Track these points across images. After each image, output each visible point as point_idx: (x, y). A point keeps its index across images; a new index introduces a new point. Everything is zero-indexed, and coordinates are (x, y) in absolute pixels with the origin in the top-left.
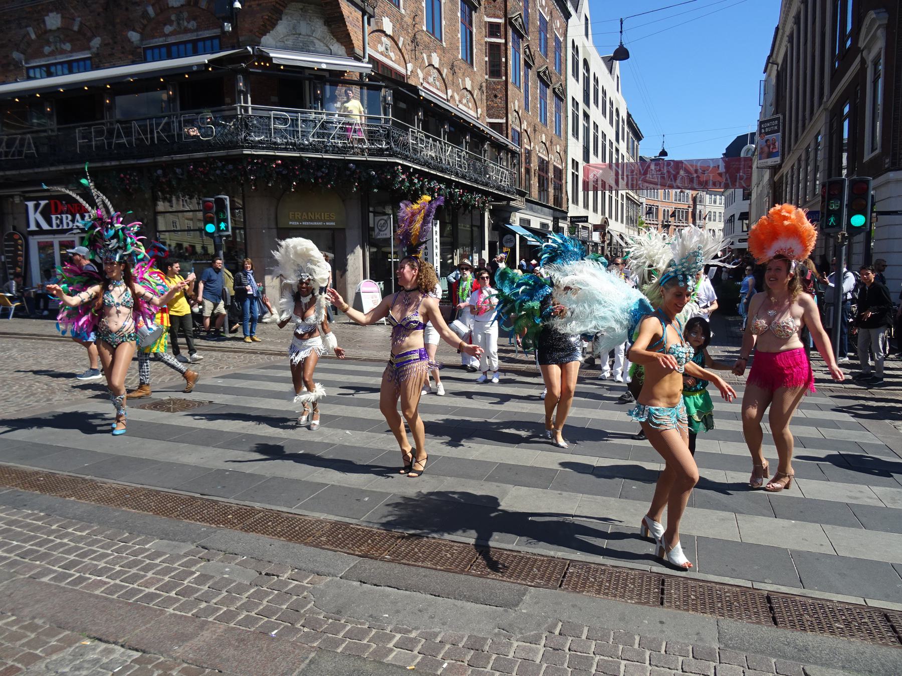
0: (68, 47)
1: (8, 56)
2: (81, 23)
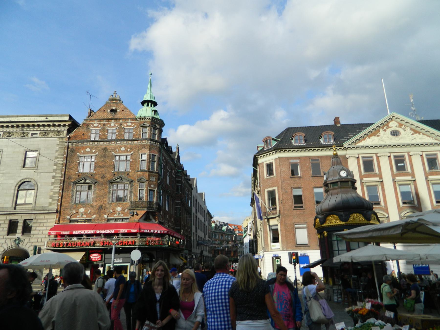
0: (85, 216)
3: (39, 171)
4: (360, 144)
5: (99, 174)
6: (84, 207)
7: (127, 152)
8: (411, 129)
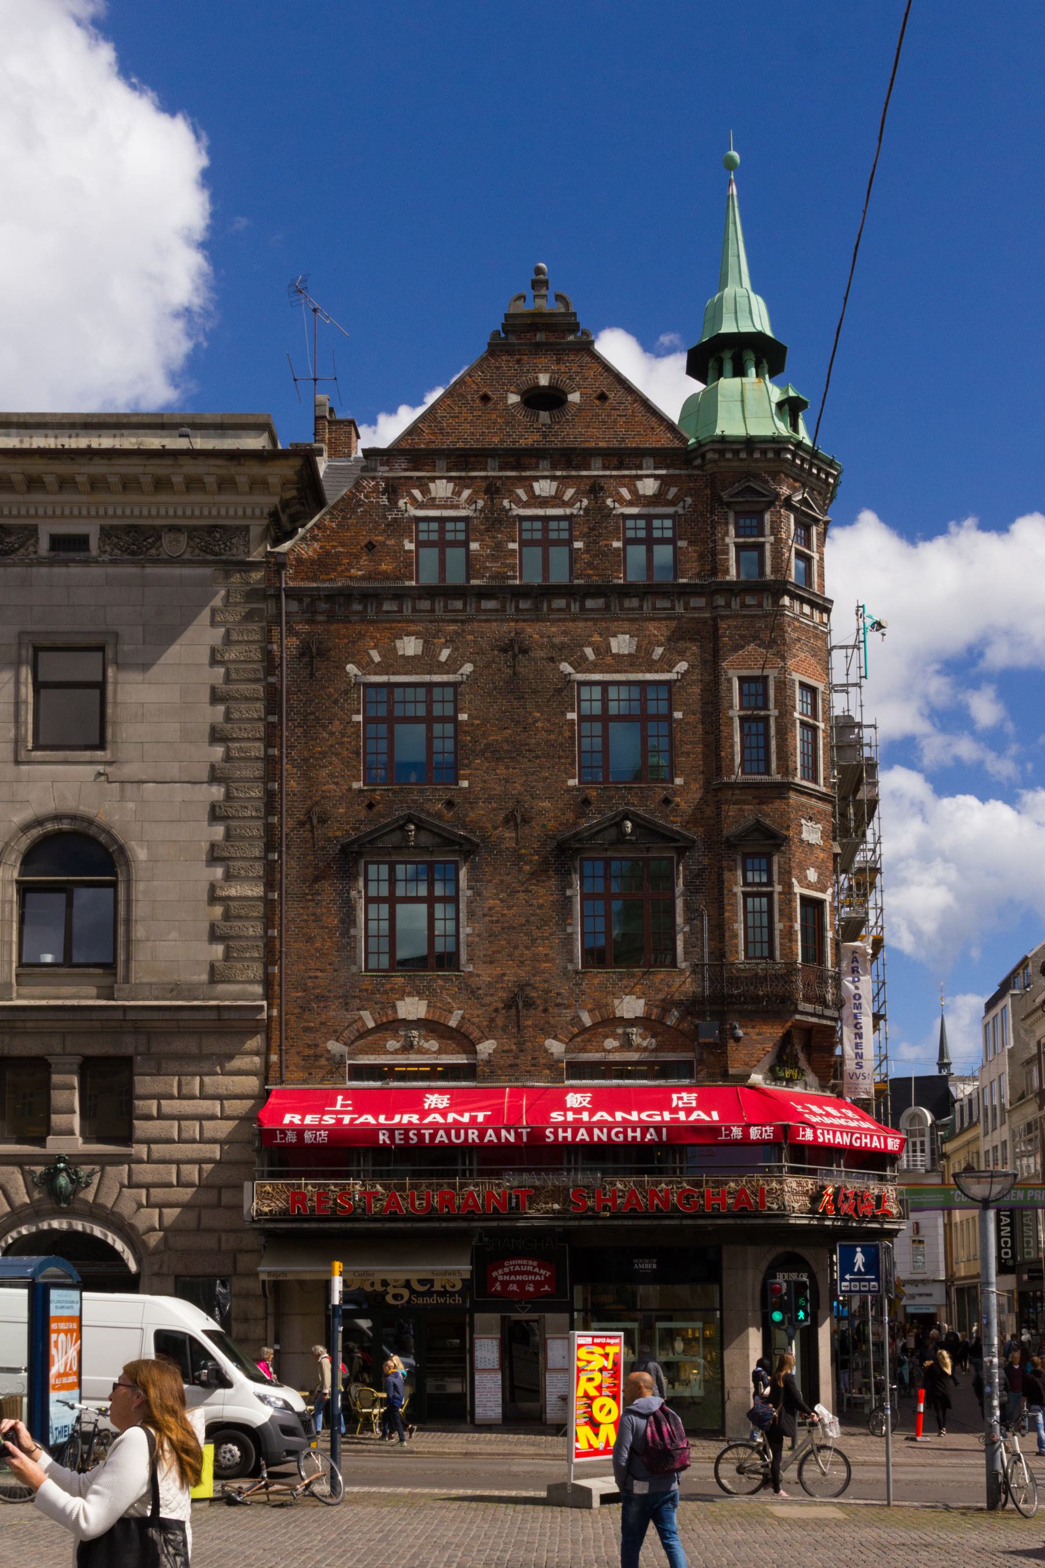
0: (433, 1045)
1: (316, 1046)
2: (463, 1018)
3: (129, 771)
5: (489, 800)
6: (420, 994)
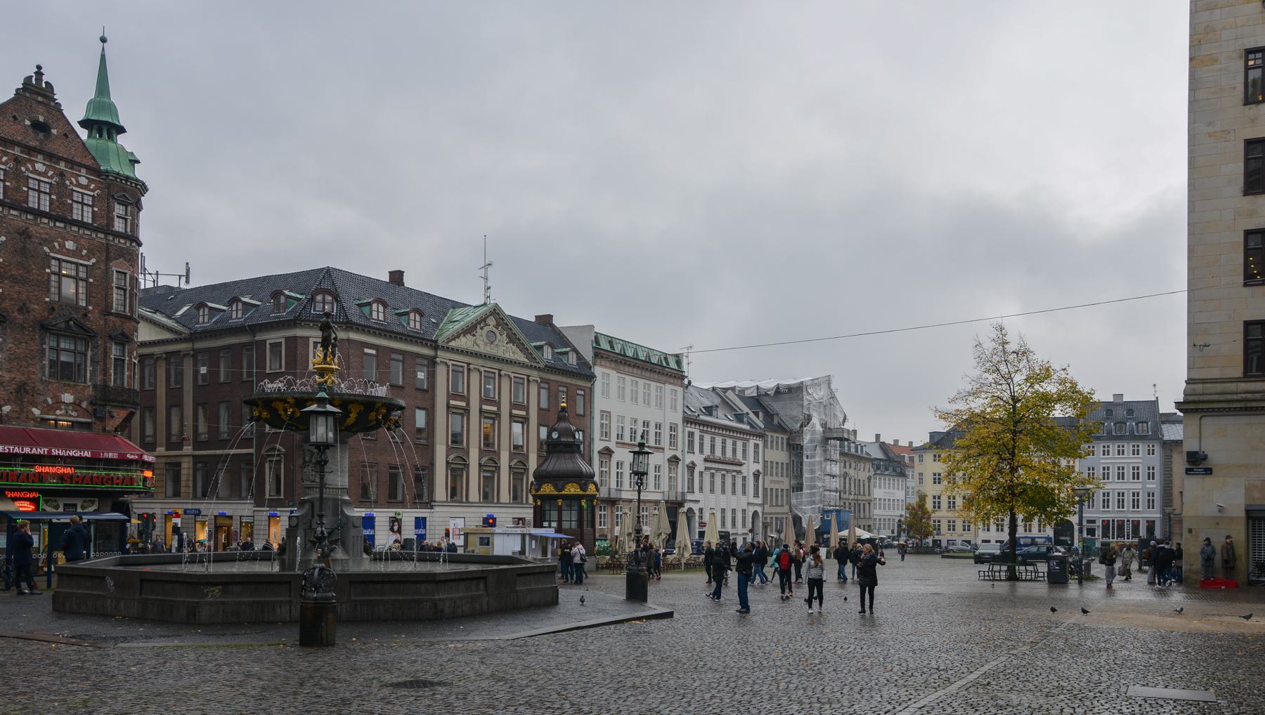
4: (453, 344)
5: (11, 299)
7: (81, 257)
8: (508, 336)
